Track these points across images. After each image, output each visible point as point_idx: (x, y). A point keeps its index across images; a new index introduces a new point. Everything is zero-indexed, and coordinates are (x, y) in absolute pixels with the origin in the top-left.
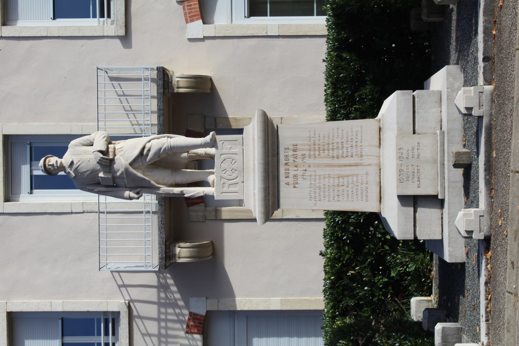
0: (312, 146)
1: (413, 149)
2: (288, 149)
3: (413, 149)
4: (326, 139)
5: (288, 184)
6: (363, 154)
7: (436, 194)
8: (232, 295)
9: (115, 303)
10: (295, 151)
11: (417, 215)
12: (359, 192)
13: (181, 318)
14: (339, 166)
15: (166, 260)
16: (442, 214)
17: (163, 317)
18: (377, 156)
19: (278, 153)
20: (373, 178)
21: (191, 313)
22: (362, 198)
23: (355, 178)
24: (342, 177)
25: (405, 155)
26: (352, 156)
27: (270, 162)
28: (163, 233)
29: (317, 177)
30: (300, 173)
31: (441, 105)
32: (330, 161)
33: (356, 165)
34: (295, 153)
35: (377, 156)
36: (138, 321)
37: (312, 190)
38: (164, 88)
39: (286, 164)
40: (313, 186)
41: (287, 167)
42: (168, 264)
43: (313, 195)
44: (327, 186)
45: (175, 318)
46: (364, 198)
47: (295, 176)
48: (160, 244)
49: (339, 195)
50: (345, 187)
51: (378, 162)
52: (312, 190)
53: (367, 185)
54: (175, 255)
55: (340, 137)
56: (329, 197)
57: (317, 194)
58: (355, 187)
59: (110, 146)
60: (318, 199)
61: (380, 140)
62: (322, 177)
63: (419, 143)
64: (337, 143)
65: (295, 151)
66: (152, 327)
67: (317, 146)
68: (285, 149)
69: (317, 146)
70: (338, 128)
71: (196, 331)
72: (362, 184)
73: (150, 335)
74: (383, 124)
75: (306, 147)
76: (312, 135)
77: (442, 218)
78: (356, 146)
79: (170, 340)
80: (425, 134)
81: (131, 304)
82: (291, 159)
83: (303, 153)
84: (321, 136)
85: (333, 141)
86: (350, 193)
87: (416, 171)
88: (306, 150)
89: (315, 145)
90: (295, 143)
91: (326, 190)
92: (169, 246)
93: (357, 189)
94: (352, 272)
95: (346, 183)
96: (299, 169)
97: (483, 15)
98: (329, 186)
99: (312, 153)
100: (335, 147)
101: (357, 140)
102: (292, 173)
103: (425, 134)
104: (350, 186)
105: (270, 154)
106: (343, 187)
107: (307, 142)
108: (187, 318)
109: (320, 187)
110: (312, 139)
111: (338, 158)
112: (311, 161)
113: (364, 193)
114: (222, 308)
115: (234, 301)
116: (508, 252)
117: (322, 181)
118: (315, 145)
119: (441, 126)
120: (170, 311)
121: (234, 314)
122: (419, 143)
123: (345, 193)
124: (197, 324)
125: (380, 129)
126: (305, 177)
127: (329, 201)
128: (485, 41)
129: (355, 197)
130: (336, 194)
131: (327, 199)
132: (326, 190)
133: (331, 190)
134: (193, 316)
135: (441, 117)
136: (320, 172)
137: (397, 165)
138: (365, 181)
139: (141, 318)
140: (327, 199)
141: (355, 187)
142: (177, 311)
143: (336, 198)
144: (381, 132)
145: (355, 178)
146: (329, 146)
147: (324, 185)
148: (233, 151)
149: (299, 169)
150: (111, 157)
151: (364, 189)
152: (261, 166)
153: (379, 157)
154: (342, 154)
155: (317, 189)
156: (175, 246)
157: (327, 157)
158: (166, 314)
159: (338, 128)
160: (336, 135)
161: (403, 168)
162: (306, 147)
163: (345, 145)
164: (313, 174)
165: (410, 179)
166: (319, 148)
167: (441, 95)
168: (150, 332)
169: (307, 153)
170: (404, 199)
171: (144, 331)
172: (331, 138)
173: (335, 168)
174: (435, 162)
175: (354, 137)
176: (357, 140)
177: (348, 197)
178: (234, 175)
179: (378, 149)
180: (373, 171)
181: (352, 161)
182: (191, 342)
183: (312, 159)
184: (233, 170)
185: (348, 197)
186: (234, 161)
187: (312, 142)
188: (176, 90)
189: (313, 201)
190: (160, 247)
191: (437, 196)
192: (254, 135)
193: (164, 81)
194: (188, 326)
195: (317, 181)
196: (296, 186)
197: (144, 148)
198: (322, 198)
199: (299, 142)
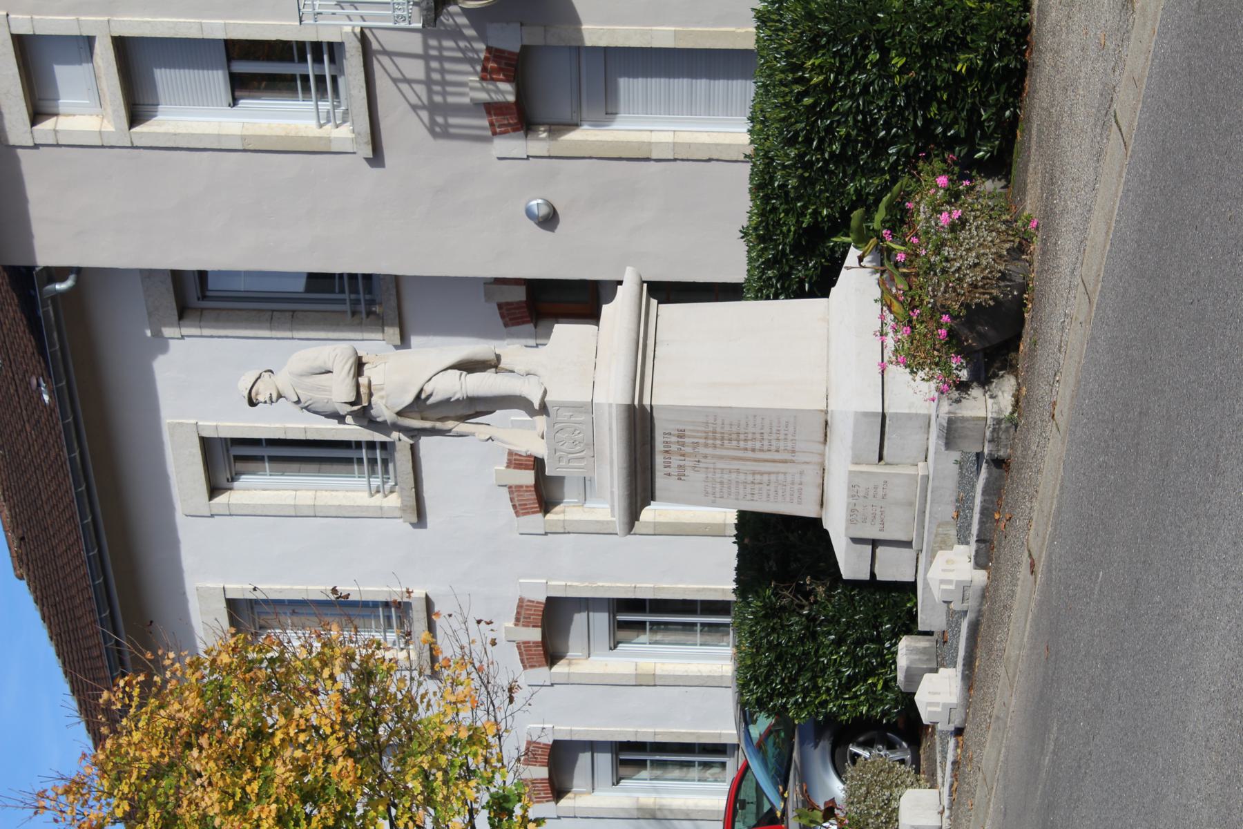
1: (876, 488)
3: (876, 488)
8: (575, 20)
9: (337, 27)
13: (470, 55)
17: (434, 53)
19: (652, 438)
21: (489, 49)
23: (781, 477)
27: (638, 456)
32: (740, 454)
33: (785, 462)
36: (385, 60)
45: (460, 55)
47: (680, 466)
59: (361, 380)
66: (415, 69)
71: (501, 77)
73: (409, 82)
79: (449, 89)
81: (367, 32)
87: (878, 512)
97: (983, 494)
108: (482, 56)
109: (722, 483)
112: (709, 451)
114: (553, 41)
115: (579, 31)
116: (1033, 523)
120: (448, 43)
121: (580, 51)
124: (503, 66)
128: (981, 523)
134: (495, 54)
136: (721, 464)
137: (849, 504)
139: (390, 54)
142: (462, 44)
145: (781, 477)
150: (365, 404)
152: (624, 473)
153: (823, 455)
158: (440, 48)
163: (766, 436)
168: (408, 76)
171: (397, 75)
174: (911, 504)
181: (777, 456)
182: (493, 96)
192: (610, 425)
194: (484, 69)
197: (422, 390)
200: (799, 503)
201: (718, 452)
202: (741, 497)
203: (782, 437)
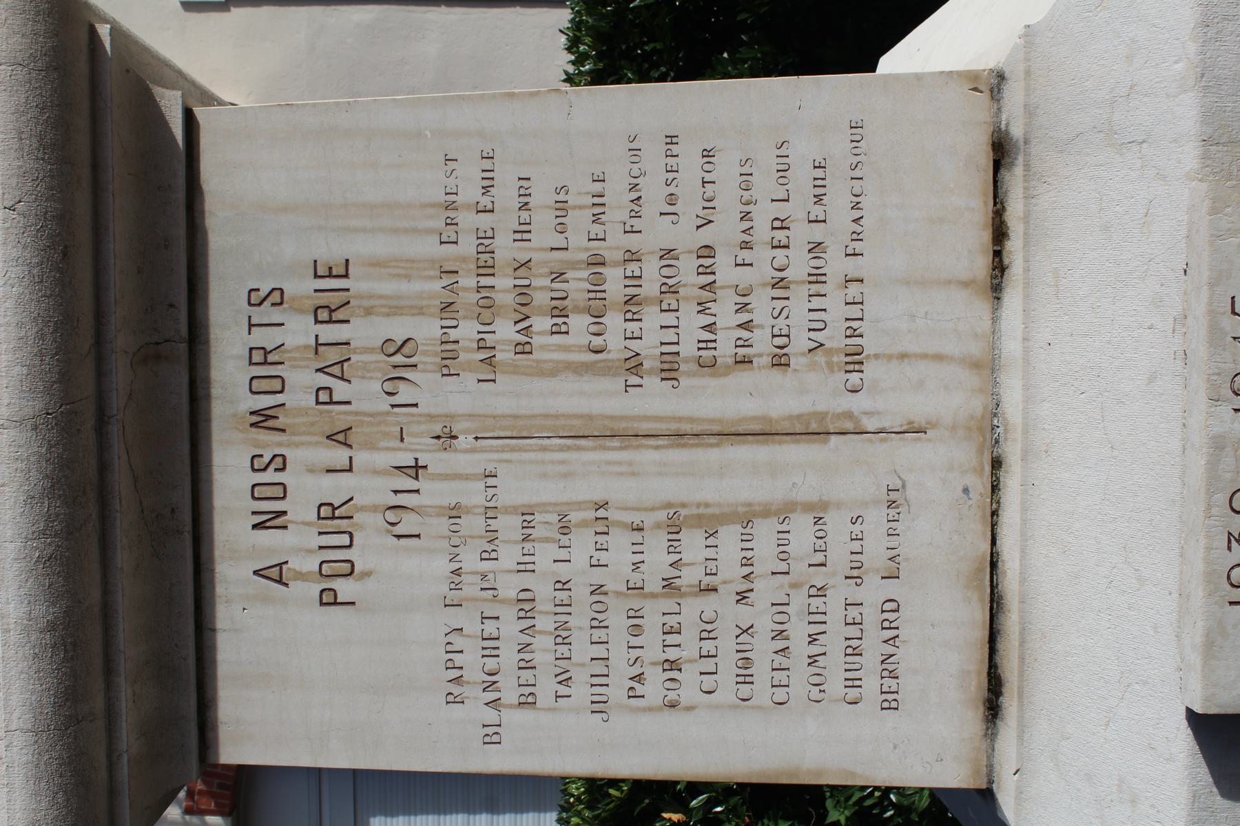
2: (277, 297)
4: (579, 221)
5: (276, 574)
6: (870, 344)
10: (327, 313)
14: (679, 437)
18: (976, 365)
20: (938, 534)
22: (853, 683)
23: (802, 532)
26: (780, 362)
27: (117, 402)
29: (508, 525)
32: (603, 398)
33: (813, 430)
34: (329, 333)
35: (976, 365)
37: (468, 620)
39: (263, 419)
40: (471, 588)
41: (269, 444)
43: (472, 661)
44: (580, 592)
46: (871, 685)
47: (330, 512)
50: (723, 606)
51: (977, 405)
52: (468, 620)
53: (891, 589)
55: (690, 207)
56: (600, 679)
57: (509, 656)
58: (799, 600)
60: (510, 694)
61: (1000, 234)
62: (545, 524)
64: (668, 253)
67: (503, 282)
68: (255, 299)
69: (503, 282)
70: (671, 140)
72: (855, 576)
75: (418, 286)
76: (470, 192)
78: (817, 277)
82: (302, 382)
83: (398, 329)
84: (542, 196)
85: (633, 241)
86: (763, 649)
88: (420, 311)
89: (486, 269)
90: (331, 250)
91: (579, 620)
93: (817, 618)
94: (676, 817)
95: (730, 570)
96: (361, 458)
98: (598, 590)
99: (467, 331)
100: (650, 287)
101: (817, 232)
102: (306, 491)
104: (766, 592)
105: (122, 340)
106: (708, 604)
107: (429, 248)
109: (525, 604)
110: (467, 219)
111: (669, 370)
112: (459, 396)
113: (873, 647)
117: (544, 556)
118: (486, 269)
123: (727, 645)
124: (214, 790)
125: (1001, 151)
126: (409, 523)
127: (599, 707)
129: (800, 674)
130: (654, 652)
131: (581, 692)
132: (579, 620)
133: (617, 621)
136: (526, 481)
138: (875, 550)
140: (581, 692)
141: (799, 600)
143: (654, 688)
144: (1014, 179)
146: (598, 281)
147: (563, 585)
149: (361, 458)
151: (871, 617)
153: (988, 366)
154: (705, 345)
155: (509, 615)
157: (580, 369)
159: (671, 140)
160: (654, 192)
162: (418, 286)
163: (726, 273)
164: (474, 494)
166: (523, 292)
169: (427, 330)
172: (616, 214)
173: (647, 456)
175: (796, 210)
176: (817, 232)
179: (982, 308)
180: (938, 474)
181: (781, 397)
183: (469, 379)
187: (468, 246)
189: (476, 711)
195: (509, 556)
196: (345, 588)
198: (546, 688)
199: (358, 248)
200: (890, 704)
201: (514, 396)
202: (617, 691)
203: (799, 266)
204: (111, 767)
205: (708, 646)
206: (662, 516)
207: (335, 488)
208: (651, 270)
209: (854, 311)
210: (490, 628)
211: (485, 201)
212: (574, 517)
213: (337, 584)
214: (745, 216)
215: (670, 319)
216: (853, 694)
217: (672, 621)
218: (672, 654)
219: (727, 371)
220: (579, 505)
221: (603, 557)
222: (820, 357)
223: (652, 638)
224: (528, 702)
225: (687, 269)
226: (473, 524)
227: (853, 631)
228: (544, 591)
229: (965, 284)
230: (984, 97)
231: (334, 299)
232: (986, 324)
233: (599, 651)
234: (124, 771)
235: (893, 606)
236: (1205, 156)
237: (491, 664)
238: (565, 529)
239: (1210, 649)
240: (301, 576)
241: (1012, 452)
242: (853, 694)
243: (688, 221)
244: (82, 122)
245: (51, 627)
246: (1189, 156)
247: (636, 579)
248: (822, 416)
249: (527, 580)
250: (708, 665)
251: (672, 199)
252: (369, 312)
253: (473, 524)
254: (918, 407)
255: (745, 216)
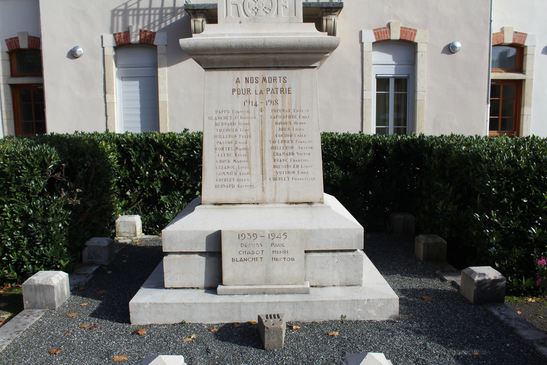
0: (288, 114)
1: (284, 252)
2: (285, 82)
3: (284, 252)
4: (298, 133)
5: (238, 81)
6: (278, 182)
7: (224, 282)
8: (169, 64)
10: (282, 90)
11: (197, 256)
12: (227, 176)
13: (152, 26)
15: (192, 10)
16: (198, 288)
17: (152, 12)
18: (274, 200)
19: (278, 68)
20: (245, 194)
21: (155, 33)
22: (220, 180)
23: (246, 171)
24: (248, 153)
25: (276, 241)
26: (274, 167)
27: (267, 56)
28: (213, 8)
29: (246, 121)
30: (253, 97)
31: (342, 286)
32: (268, 137)
34: (279, 91)
35: (274, 200)
37: (230, 114)
38: (326, 8)
39: (264, 79)
40: (236, 115)
41: (260, 80)
42: (189, 12)
43: (223, 115)
44: (235, 133)
45: (152, 21)
46: (220, 183)
47: (249, 91)
48: (204, 5)
49: (223, 149)
50: (233, 157)
51: (268, 200)
52: (230, 114)
53: (236, 186)
54: (197, 18)
55: (300, 151)
56: (220, 137)
57: (224, 121)
58: (234, 170)
60: (218, 121)
61: (296, 203)
62: (247, 127)
63: (293, 259)
65: (282, 90)
69: (288, 120)
70: (312, 148)
74: (316, 207)
75: (287, 105)
76: (303, 114)
77: (193, 288)
78: (289, 173)
79: (135, 17)
80: (305, 266)
82: (271, 86)
83: (280, 102)
84: (302, 126)
85: (295, 141)
86: (226, 164)
87: (255, 256)
88: (283, 106)
89: (290, 117)
90: (293, 91)
91: (230, 133)
92: (204, 13)
93: (231, 174)
94: (162, 160)
95: (239, 158)
98: (236, 136)
99: (279, 114)
100: (287, 145)
101: (296, 173)
102: (252, 87)
103: (305, 266)
104: (236, 165)
105: (277, 57)
106: (233, 155)
107: (293, 107)
108: (152, 30)
110: (298, 114)
111: (273, 148)
113: (226, 183)
114: (159, 57)
115: (164, 66)
117: (241, 127)
118: (290, 117)
119: (316, 287)
120: (157, 17)
121: (155, 67)
122: (293, 259)
123: (226, 158)
125: (310, 203)
126: (247, 104)
127: (215, 137)
129: (221, 171)
131: (218, 133)
132: (230, 133)
133: (230, 140)
134: (153, 35)
135: (327, 286)
136: (254, 124)
137: (264, 231)
140: (218, 133)
141: (234, 170)
142: (157, 23)
144: (306, 205)
146: (288, 136)
147: (236, 130)
148: (281, 9)
149: (258, 96)
151: (231, 183)
153: (274, 202)
154: (277, 154)
155: (231, 121)
156: (203, 17)
157: (273, 133)
158: (155, 14)
159: (312, 148)
160: (302, 145)
161: (259, 238)
162: (287, 105)
163: (290, 157)
164: (252, 115)
165: (244, 249)
166: (286, 123)
167: (357, 285)
169: (279, 107)
170: (216, 239)
172: (299, 139)
173: (258, 144)
174: (268, 281)
176: (296, 173)
177: (220, 161)
178: (249, 11)
179: (284, 201)
180: (256, 194)
182: (134, 34)
183: (271, 114)
184: (256, 10)
185: (220, 161)
186: (268, 12)
187: (294, 114)
188: (324, 18)
189: (215, 115)
190: (202, 5)
191: (221, 283)
193: (332, 8)
194: (146, 31)
195: (241, 121)
196: (235, 93)
198: (219, 128)
202: (218, 139)
203: (291, 169)
204: (206, 55)
205: (226, 155)
206: (248, 147)
207: (253, 91)
208: (290, 145)
209: (283, 179)
210: (229, 118)
211: (301, 117)
212: (248, 132)
213: (236, 92)
214: (299, 160)
215: (282, 148)
216: (218, 180)
217: (230, 149)
218: (225, 149)
219: (273, 158)
220: (250, 133)
221: (241, 137)
222: (276, 173)
223: (227, 145)
224: (216, 124)
225: (290, 151)
226: (247, 115)
227: (229, 180)
228: (235, 127)
229: (288, 198)
230: (319, 200)
231: (285, 91)
232: (281, 202)
233: (225, 136)
234: (205, 57)
235: (233, 186)
236: (308, 230)
237: (223, 118)
238: (246, 130)
239: (232, 231)
240: (238, 85)
241: (260, 206)
242: (218, 180)
243: (298, 151)
244: (313, 51)
245: (231, 46)
246: (308, 228)
247: (237, 143)
248: (265, 174)
249: (237, 124)
250: (223, 155)
251: (302, 148)
252: (283, 97)
253: (247, 115)
254: (267, 190)
255: (299, 160)
